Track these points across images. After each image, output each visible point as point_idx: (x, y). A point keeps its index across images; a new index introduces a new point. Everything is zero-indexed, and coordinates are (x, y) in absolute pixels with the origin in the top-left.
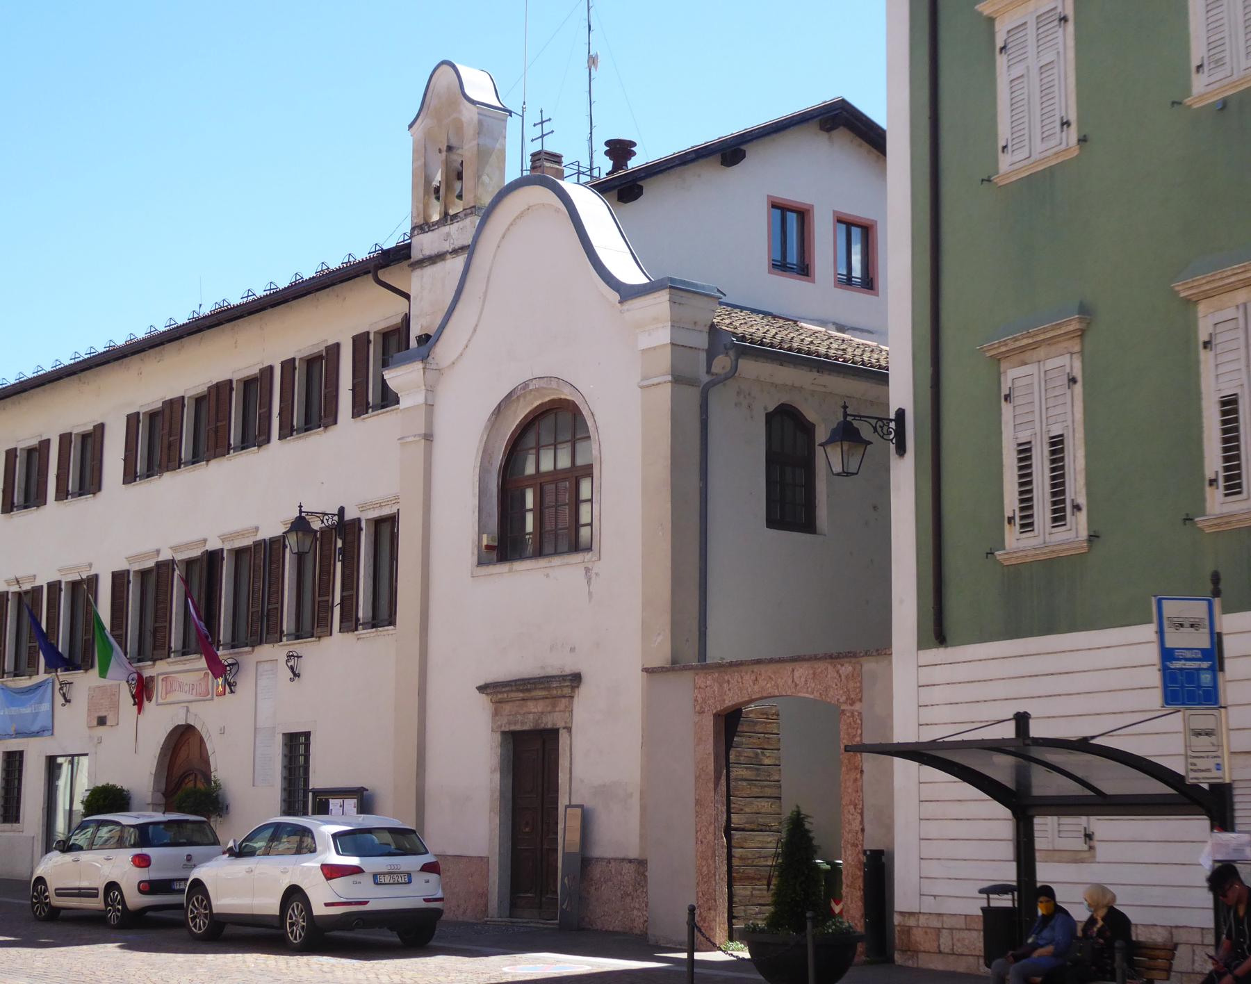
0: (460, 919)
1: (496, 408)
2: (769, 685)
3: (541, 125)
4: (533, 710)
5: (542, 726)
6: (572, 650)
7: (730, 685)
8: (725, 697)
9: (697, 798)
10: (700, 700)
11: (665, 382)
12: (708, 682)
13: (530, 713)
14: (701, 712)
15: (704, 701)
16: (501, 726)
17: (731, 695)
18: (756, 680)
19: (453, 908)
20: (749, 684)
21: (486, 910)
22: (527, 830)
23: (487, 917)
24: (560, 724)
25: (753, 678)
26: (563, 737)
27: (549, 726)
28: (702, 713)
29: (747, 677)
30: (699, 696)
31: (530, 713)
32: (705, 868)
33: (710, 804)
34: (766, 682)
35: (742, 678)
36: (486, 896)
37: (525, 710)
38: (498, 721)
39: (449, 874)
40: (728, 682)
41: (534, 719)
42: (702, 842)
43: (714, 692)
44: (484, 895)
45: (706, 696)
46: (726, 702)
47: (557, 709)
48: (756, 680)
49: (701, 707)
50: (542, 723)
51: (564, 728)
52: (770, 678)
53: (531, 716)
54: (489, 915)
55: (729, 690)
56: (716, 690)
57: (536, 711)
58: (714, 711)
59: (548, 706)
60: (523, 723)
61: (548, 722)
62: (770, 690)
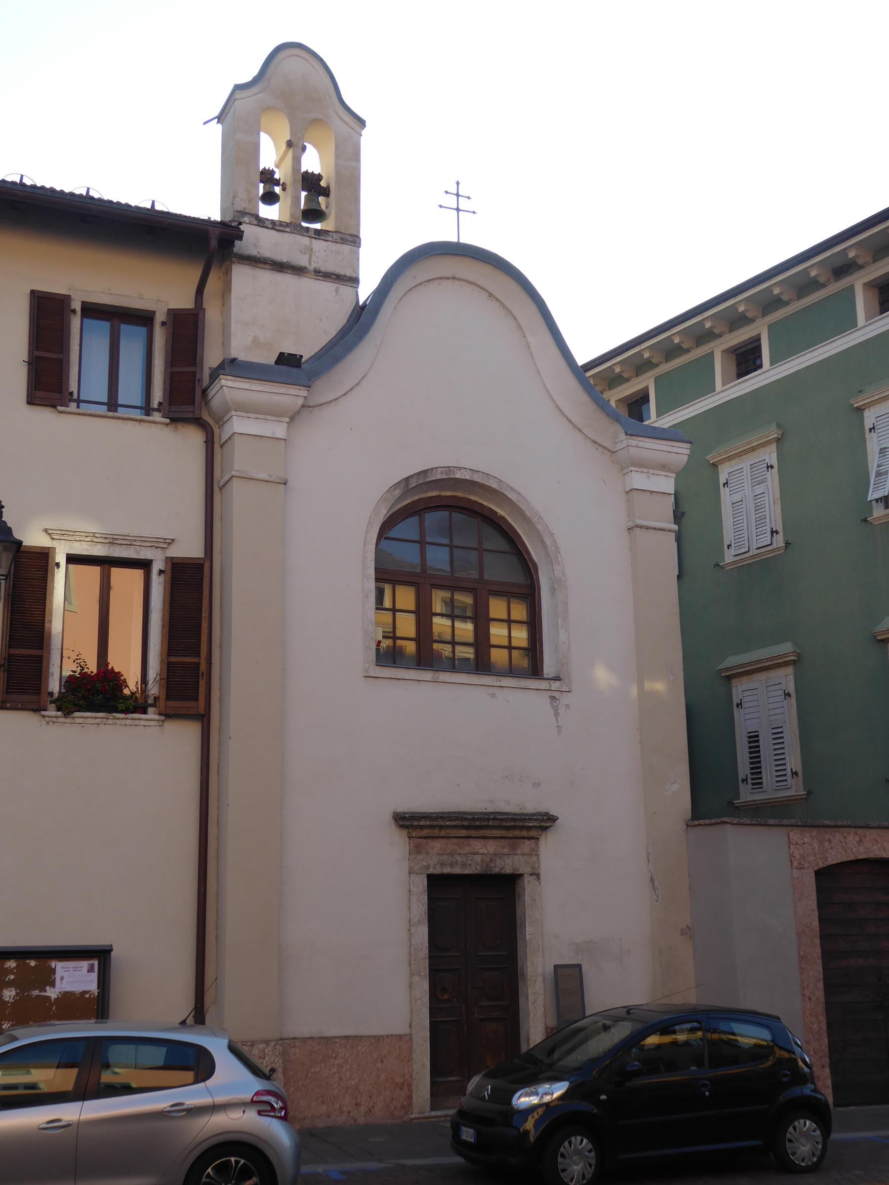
0: (362, 1120)
1: (399, 483)
2: (875, 847)
3: (460, 198)
4: (481, 851)
5: (496, 870)
6: (536, 785)
7: (832, 845)
8: (827, 855)
9: (802, 953)
10: (798, 857)
11: (669, 531)
12: (806, 839)
13: (477, 854)
14: (801, 868)
15: (803, 857)
16: (428, 867)
17: (833, 853)
18: (861, 841)
19: (345, 1108)
20: (853, 844)
21: (410, 1104)
22: (445, 997)
23: (412, 1113)
24: (524, 869)
25: (857, 838)
26: (528, 886)
27: (508, 870)
28: (800, 869)
29: (851, 838)
30: (796, 851)
31: (477, 854)
32: (816, 1026)
33: (817, 960)
34: (871, 844)
35: (845, 838)
36: (409, 1085)
37: (467, 849)
38: (423, 860)
39: (337, 1062)
40: (830, 841)
41: (482, 861)
42: (810, 999)
43: (814, 849)
44: (407, 1085)
45: (804, 852)
46: (829, 860)
47: (519, 852)
48: (861, 841)
49: (800, 864)
50: (495, 867)
51: (531, 875)
52: (876, 840)
53: (478, 858)
54: (415, 1111)
55: (832, 848)
56: (817, 847)
57: (486, 852)
58: (816, 869)
59: (504, 847)
60: (464, 865)
61: (507, 865)
62: (877, 852)
